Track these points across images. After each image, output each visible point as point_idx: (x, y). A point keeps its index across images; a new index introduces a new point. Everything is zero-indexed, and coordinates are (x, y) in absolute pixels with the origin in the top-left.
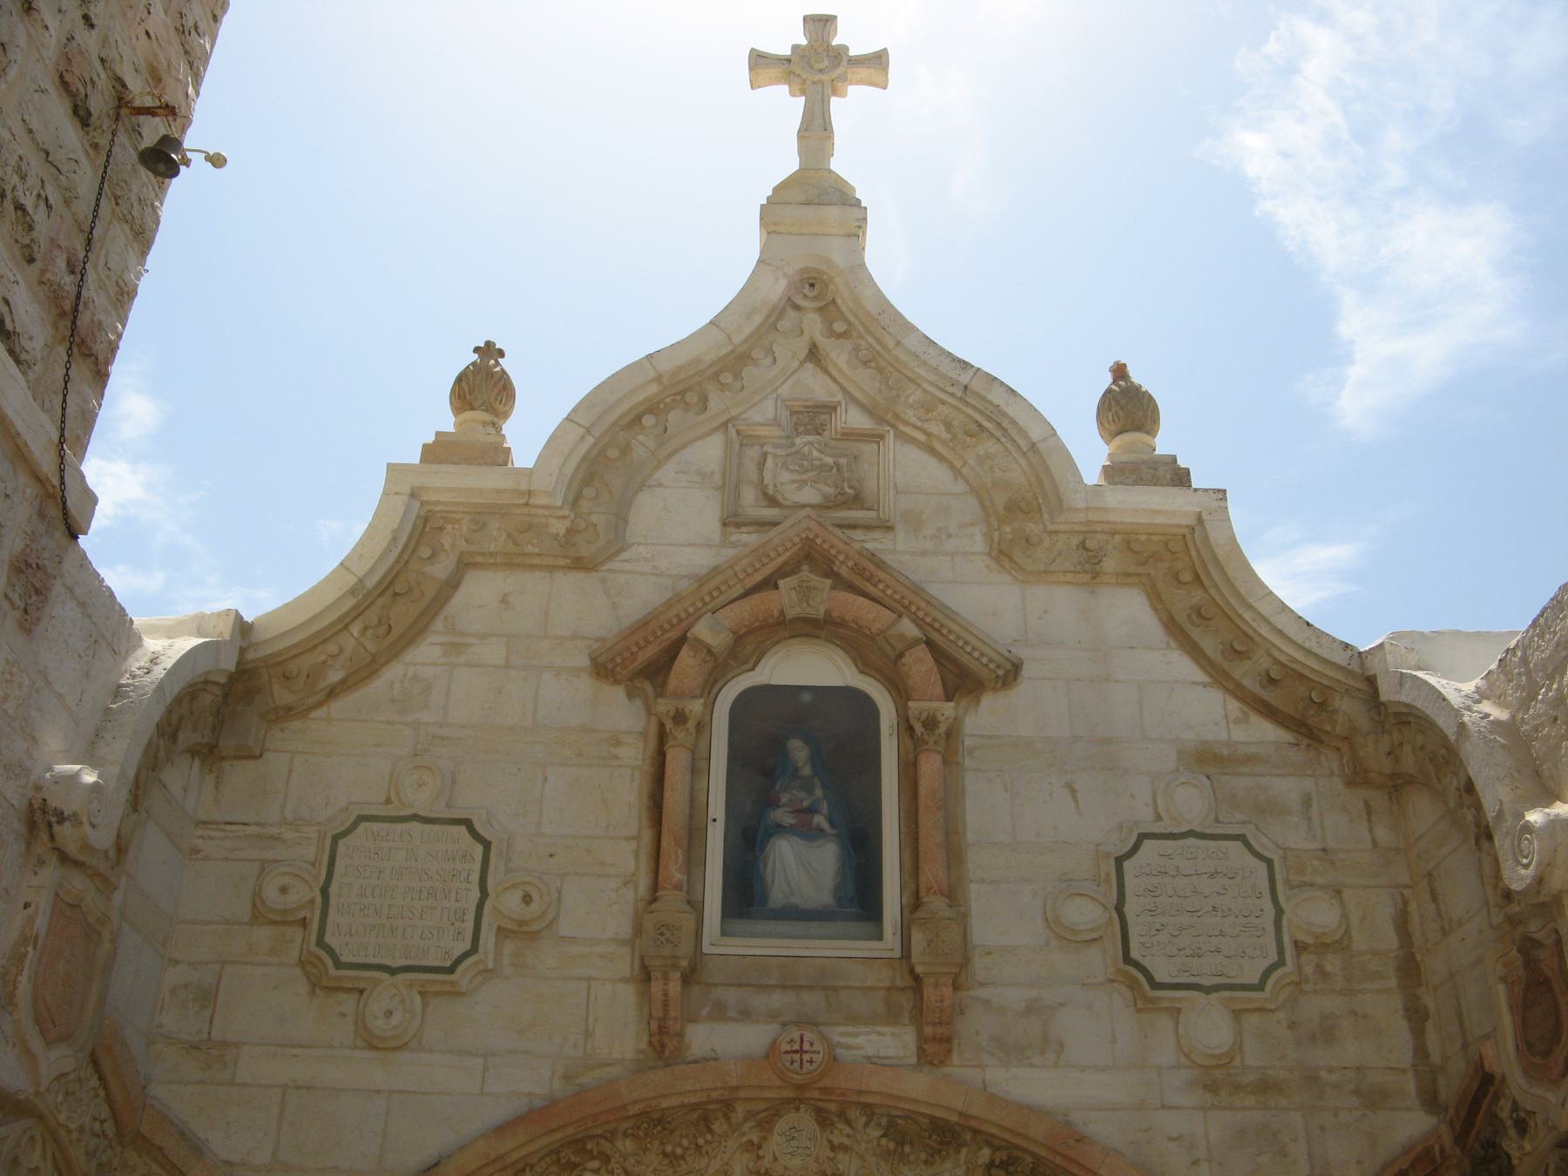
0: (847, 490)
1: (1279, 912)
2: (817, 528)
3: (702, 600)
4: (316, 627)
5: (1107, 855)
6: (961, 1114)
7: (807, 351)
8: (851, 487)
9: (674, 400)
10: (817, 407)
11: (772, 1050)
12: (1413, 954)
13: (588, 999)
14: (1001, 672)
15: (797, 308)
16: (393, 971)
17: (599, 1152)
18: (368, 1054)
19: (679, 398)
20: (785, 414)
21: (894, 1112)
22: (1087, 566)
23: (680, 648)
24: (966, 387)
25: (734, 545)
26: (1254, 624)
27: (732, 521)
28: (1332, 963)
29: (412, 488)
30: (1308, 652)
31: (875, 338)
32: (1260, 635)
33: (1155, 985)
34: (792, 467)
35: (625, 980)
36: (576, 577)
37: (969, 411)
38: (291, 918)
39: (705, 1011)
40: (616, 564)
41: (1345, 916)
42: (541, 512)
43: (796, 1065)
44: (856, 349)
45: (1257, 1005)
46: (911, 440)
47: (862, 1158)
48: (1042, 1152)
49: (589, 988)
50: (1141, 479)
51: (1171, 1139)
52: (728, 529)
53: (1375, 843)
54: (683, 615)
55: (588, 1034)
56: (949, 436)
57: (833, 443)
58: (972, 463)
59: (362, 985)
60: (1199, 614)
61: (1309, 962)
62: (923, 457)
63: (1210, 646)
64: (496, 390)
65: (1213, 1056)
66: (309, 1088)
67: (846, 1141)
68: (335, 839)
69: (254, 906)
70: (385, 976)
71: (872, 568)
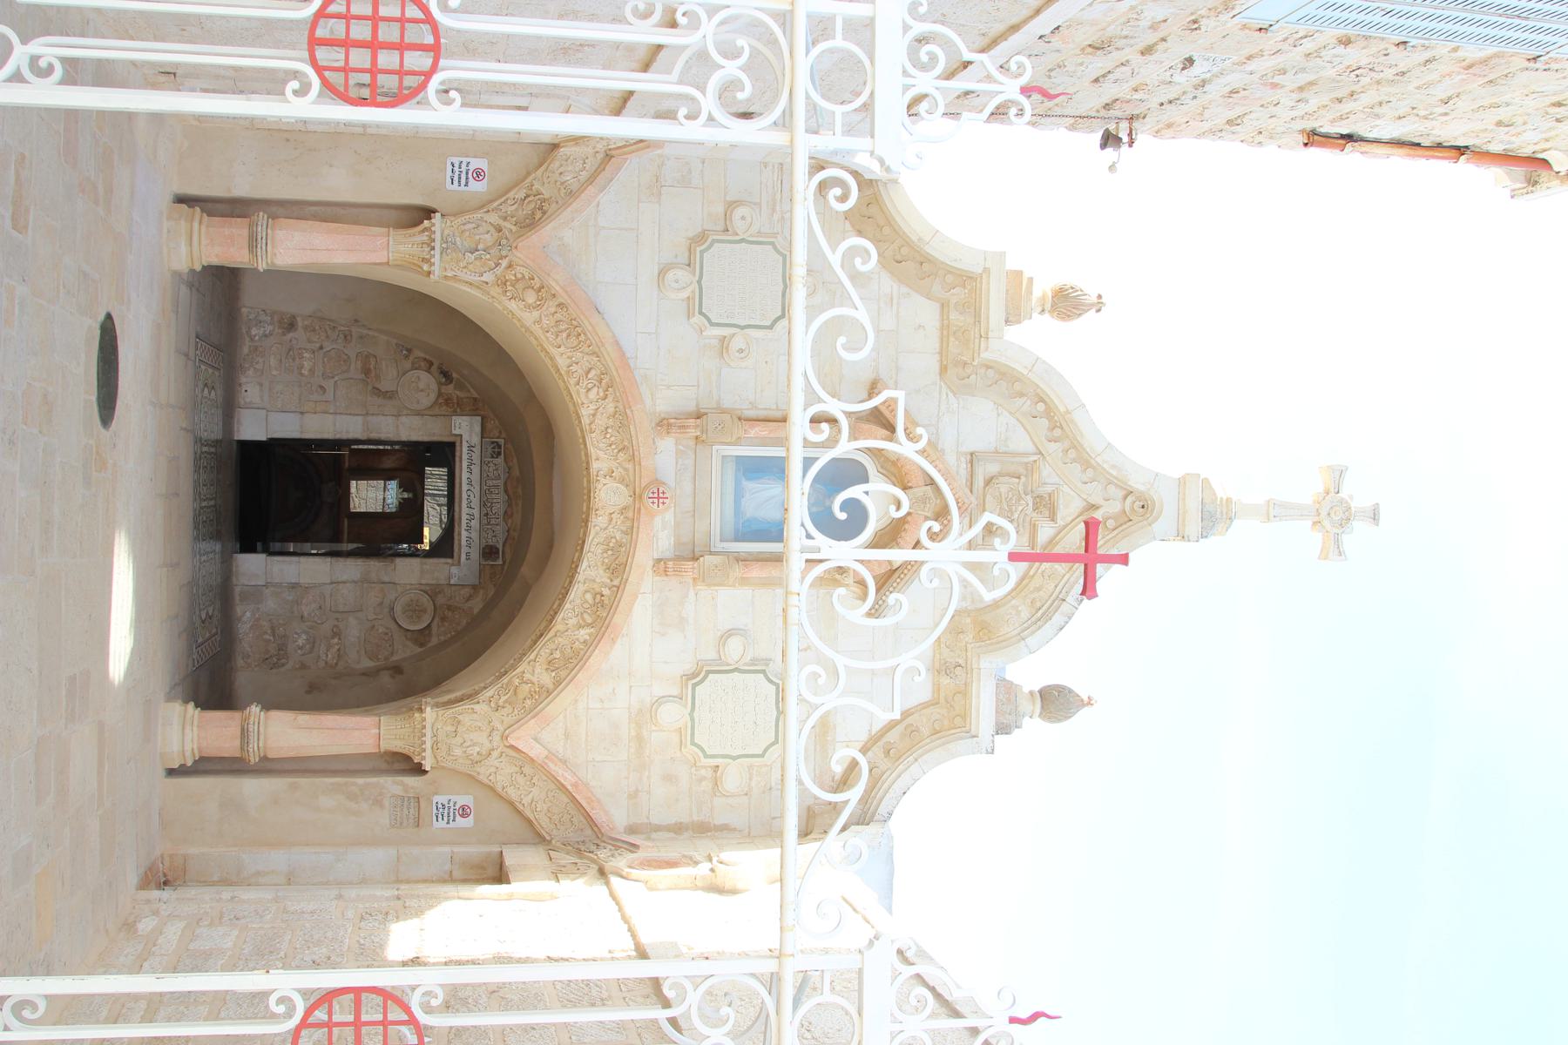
1: (734, 758)
4: (898, 219)
5: (767, 665)
6: (627, 580)
7: (1093, 503)
9: (1056, 421)
15: (1125, 498)
16: (699, 282)
18: (656, 272)
20: (1049, 489)
22: (944, 668)
25: (958, 459)
26: (906, 762)
28: (707, 785)
32: (899, 765)
33: (695, 686)
35: (697, 405)
36: (936, 367)
37: (1049, 602)
39: (681, 447)
40: (944, 390)
41: (733, 796)
43: (651, 495)
47: (606, 529)
52: (969, 457)
53: (774, 818)
55: (668, 387)
56: (1031, 589)
57: (1028, 519)
58: (1013, 602)
60: (912, 731)
61: (709, 773)
63: (892, 736)
64: (1065, 311)
65: (656, 715)
67: (614, 521)
68: (772, 244)
69: (735, 202)
70: (697, 278)
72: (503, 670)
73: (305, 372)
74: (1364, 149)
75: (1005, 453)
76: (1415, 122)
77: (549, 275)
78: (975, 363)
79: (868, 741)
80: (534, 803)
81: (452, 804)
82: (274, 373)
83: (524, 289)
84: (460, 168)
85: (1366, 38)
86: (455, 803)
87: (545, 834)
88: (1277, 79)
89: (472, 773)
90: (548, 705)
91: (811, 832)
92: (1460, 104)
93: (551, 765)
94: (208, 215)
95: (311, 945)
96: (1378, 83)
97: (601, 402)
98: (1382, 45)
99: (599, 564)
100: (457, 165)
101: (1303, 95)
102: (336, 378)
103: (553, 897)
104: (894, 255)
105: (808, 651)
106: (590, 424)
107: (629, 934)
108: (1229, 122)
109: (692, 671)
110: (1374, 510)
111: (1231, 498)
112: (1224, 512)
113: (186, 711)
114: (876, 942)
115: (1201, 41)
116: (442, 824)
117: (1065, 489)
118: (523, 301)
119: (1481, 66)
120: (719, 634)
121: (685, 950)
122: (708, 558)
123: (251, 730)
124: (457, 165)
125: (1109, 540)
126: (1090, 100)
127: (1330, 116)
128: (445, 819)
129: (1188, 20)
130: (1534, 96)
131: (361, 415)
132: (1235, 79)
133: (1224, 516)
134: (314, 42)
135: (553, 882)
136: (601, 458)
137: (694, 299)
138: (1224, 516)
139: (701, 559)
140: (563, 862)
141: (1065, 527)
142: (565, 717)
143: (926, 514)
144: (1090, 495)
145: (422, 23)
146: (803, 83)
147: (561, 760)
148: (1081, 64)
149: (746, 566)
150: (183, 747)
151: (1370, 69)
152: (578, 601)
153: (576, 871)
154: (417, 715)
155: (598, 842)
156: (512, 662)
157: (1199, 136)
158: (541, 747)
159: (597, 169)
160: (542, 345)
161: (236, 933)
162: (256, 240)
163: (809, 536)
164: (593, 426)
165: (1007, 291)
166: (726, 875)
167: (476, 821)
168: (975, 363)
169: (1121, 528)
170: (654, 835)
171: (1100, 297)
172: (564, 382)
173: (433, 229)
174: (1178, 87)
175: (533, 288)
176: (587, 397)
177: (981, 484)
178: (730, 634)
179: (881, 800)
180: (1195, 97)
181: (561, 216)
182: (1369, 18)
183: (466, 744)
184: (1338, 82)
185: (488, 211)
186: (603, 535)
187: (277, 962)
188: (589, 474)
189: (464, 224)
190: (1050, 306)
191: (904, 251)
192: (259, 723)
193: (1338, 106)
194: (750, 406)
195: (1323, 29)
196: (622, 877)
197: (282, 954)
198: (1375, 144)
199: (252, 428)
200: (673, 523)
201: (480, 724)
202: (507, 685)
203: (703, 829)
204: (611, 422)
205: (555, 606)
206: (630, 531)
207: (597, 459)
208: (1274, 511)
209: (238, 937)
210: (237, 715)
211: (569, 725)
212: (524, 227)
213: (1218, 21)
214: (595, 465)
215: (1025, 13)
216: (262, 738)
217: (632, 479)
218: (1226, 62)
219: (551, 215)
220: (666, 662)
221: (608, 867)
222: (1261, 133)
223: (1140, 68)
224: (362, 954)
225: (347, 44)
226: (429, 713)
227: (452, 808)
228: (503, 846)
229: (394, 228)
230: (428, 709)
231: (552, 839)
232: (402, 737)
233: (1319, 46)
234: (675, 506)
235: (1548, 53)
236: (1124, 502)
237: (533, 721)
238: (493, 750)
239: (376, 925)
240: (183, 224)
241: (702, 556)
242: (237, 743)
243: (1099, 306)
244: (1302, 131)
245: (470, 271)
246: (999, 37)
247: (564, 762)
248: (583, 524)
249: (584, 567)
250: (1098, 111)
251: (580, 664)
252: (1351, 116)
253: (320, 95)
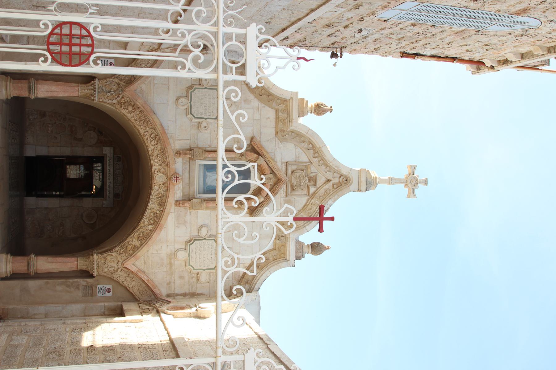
0: (295, 188)
1: (204, 270)
2: (284, 182)
3: (268, 159)
6: (166, 208)
7: (329, 179)
8: (296, 188)
9: (316, 151)
10: (315, 181)
11: (176, 174)
12: (196, 296)
15: (340, 177)
16: (190, 103)
17: (158, 143)
19: (317, 152)
20: (314, 174)
21: (166, 196)
22: (277, 237)
23: (257, 154)
25: (282, 164)
26: (264, 270)
28: (195, 280)
29: (293, 98)
30: (258, 280)
31: (332, 194)
34: (300, 176)
35: (190, 146)
36: (274, 132)
37: (314, 214)
39: (184, 161)
42: (288, 124)
43: (174, 178)
44: (329, 190)
45: (186, 265)
46: (307, 202)
47: (158, 190)
48: (159, 223)
49: (188, 139)
50: (298, 249)
51: (161, 246)
52: (286, 163)
54: (264, 155)
55: (180, 140)
56: (308, 209)
57: (306, 185)
58: (302, 214)
59: (188, 97)
61: (195, 275)
62: (304, 204)
66: (168, 88)
67: (161, 187)
71: (275, 193)
72: (122, 240)
73: (49, 132)
74: (422, 58)
75: (298, 162)
76: (438, 50)
77: (137, 100)
78: (288, 131)
79: (251, 263)
80: (133, 287)
81: (104, 288)
82: (38, 132)
83: (128, 105)
84: (104, 62)
85: (421, 24)
86: (105, 287)
87: (137, 297)
88: (391, 36)
89: (111, 277)
90: (138, 252)
91: (231, 295)
92: (453, 44)
93: (139, 274)
94: (13, 79)
95: (54, 342)
96: (426, 38)
97: (156, 145)
98: (427, 26)
99: (156, 203)
100: (103, 61)
101: (400, 41)
102: (61, 134)
103: (141, 321)
104: (259, 93)
105: (230, 232)
106: (152, 153)
107: (167, 334)
108: (375, 49)
109: (189, 239)
110: (426, 180)
111: (377, 177)
112: (374, 181)
113: (7, 256)
114: (249, 351)
115: (364, 24)
116: (101, 295)
117: (319, 174)
118: (128, 110)
119: (460, 33)
120: (198, 226)
121: (187, 340)
122: (194, 201)
123: (31, 263)
124: (103, 61)
125: (335, 192)
126: (327, 42)
127: (409, 48)
128: (102, 293)
129: (360, 17)
130: (478, 42)
131: (70, 147)
132: (377, 36)
133: (375, 183)
134: (49, 43)
135: (140, 316)
136: (156, 166)
137: (188, 108)
138: (375, 183)
139: (192, 200)
140: (144, 308)
141: (319, 187)
142: (144, 257)
143: (271, 184)
144: (328, 176)
145: (88, 37)
146: (222, 57)
147: (143, 272)
148: (323, 31)
149: (208, 203)
150: (7, 270)
151: (423, 34)
152: (148, 216)
153: (148, 312)
154: (91, 257)
155: (156, 300)
156: (125, 237)
157: (365, 53)
158: (135, 267)
159: (153, 63)
160: (134, 125)
161: (27, 337)
162: (31, 88)
163: (225, 213)
164: (153, 154)
165: (299, 105)
166: (201, 312)
167: (113, 294)
168: (288, 131)
169: (338, 188)
170: (176, 297)
171: (331, 107)
172: (143, 138)
173: (95, 84)
174: (357, 38)
175: (131, 105)
176: (151, 144)
177: (290, 173)
178: (202, 227)
179: (256, 284)
180: (363, 41)
181: (141, 80)
182: (422, 18)
183: (109, 267)
184: (412, 37)
185: (115, 78)
186: (157, 192)
187: (42, 349)
188: (152, 170)
189: (106, 82)
190: (314, 110)
191: (263, 91)
192: (34, 261)
193: (412, 45)
194: (209, 146)
195: (406, 21)
196: (165, 313)
197: (44, 345)
198: (425, 57)
199: (30, 152)
200: (182, 188)
201: (114, 260)
202: (123, 246)
203: (193, 295)
204: (159, 152)
205: (140, 218)
206: (167, 191)
207: (155, 166)
208: (391, 181)
209: (27, 339)
210: (26, 258)
211: (145, 259)
212: (128, 83)
213: (370, 18)
214: (154, 168)
215: (303, 15)
216: (35, 266)
217: (167, 172)
218: (373, 31)
219: (137, 79)
220: (179, 237)
221: (160, 309)
222: (386, 52)
223: (344, 32)
224: (72, 344)
225: (61, 44)
226: (96, 256)
227: (104, 289)
228: (123, 302)
229: (81, 84)
230: (95, 255)
231: (140, 299)
232: (86, 265)
233: (405, 26)
234: (182, 182)
235: (482, 29)
236: (340, 179)
237: (133, 258)
238: (119, 269)
239: (78, 333)
240: (4, 83)
241: (192, 199)
242: (26, 268)
243: (331, 110)
244: (400, 52)
245: (109, 99)
246: (294, 22)
247: (144, 272)
248: (150, 188)
249: (150, 204)
250: (330, 45)
251: (149, 238)
252: (417, 48)
253: (52, 62)
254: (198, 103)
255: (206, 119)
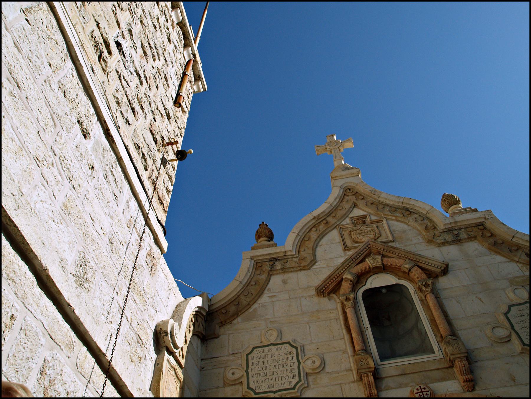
4: (230, 297)
13: (342, 390)
14: (443, 268)
24: (402, 203)
27: (346, 248)
35: (353, 382)
38: (237, 382)
42: (289, 257)
49: (341, 387)
254: (274, 379)
255: (300, 363)
